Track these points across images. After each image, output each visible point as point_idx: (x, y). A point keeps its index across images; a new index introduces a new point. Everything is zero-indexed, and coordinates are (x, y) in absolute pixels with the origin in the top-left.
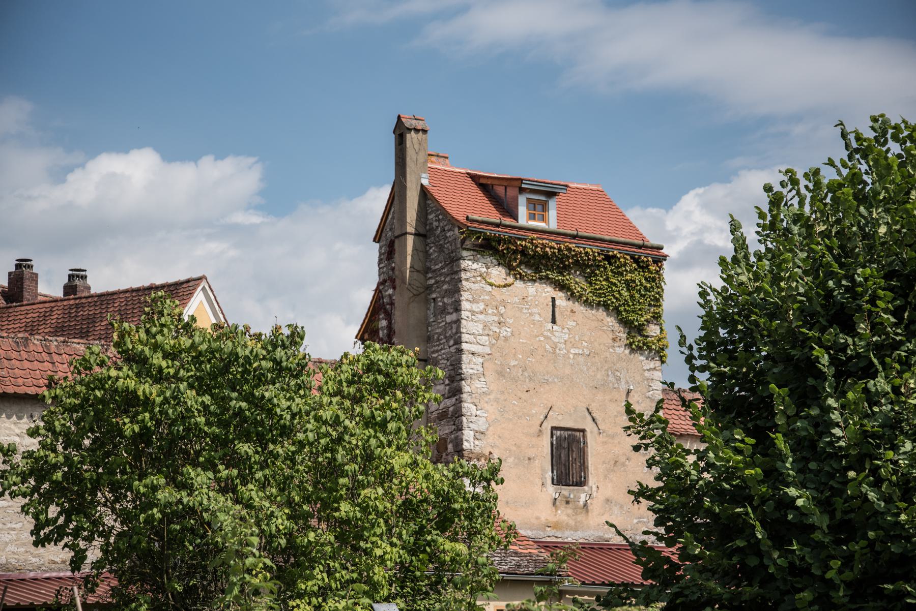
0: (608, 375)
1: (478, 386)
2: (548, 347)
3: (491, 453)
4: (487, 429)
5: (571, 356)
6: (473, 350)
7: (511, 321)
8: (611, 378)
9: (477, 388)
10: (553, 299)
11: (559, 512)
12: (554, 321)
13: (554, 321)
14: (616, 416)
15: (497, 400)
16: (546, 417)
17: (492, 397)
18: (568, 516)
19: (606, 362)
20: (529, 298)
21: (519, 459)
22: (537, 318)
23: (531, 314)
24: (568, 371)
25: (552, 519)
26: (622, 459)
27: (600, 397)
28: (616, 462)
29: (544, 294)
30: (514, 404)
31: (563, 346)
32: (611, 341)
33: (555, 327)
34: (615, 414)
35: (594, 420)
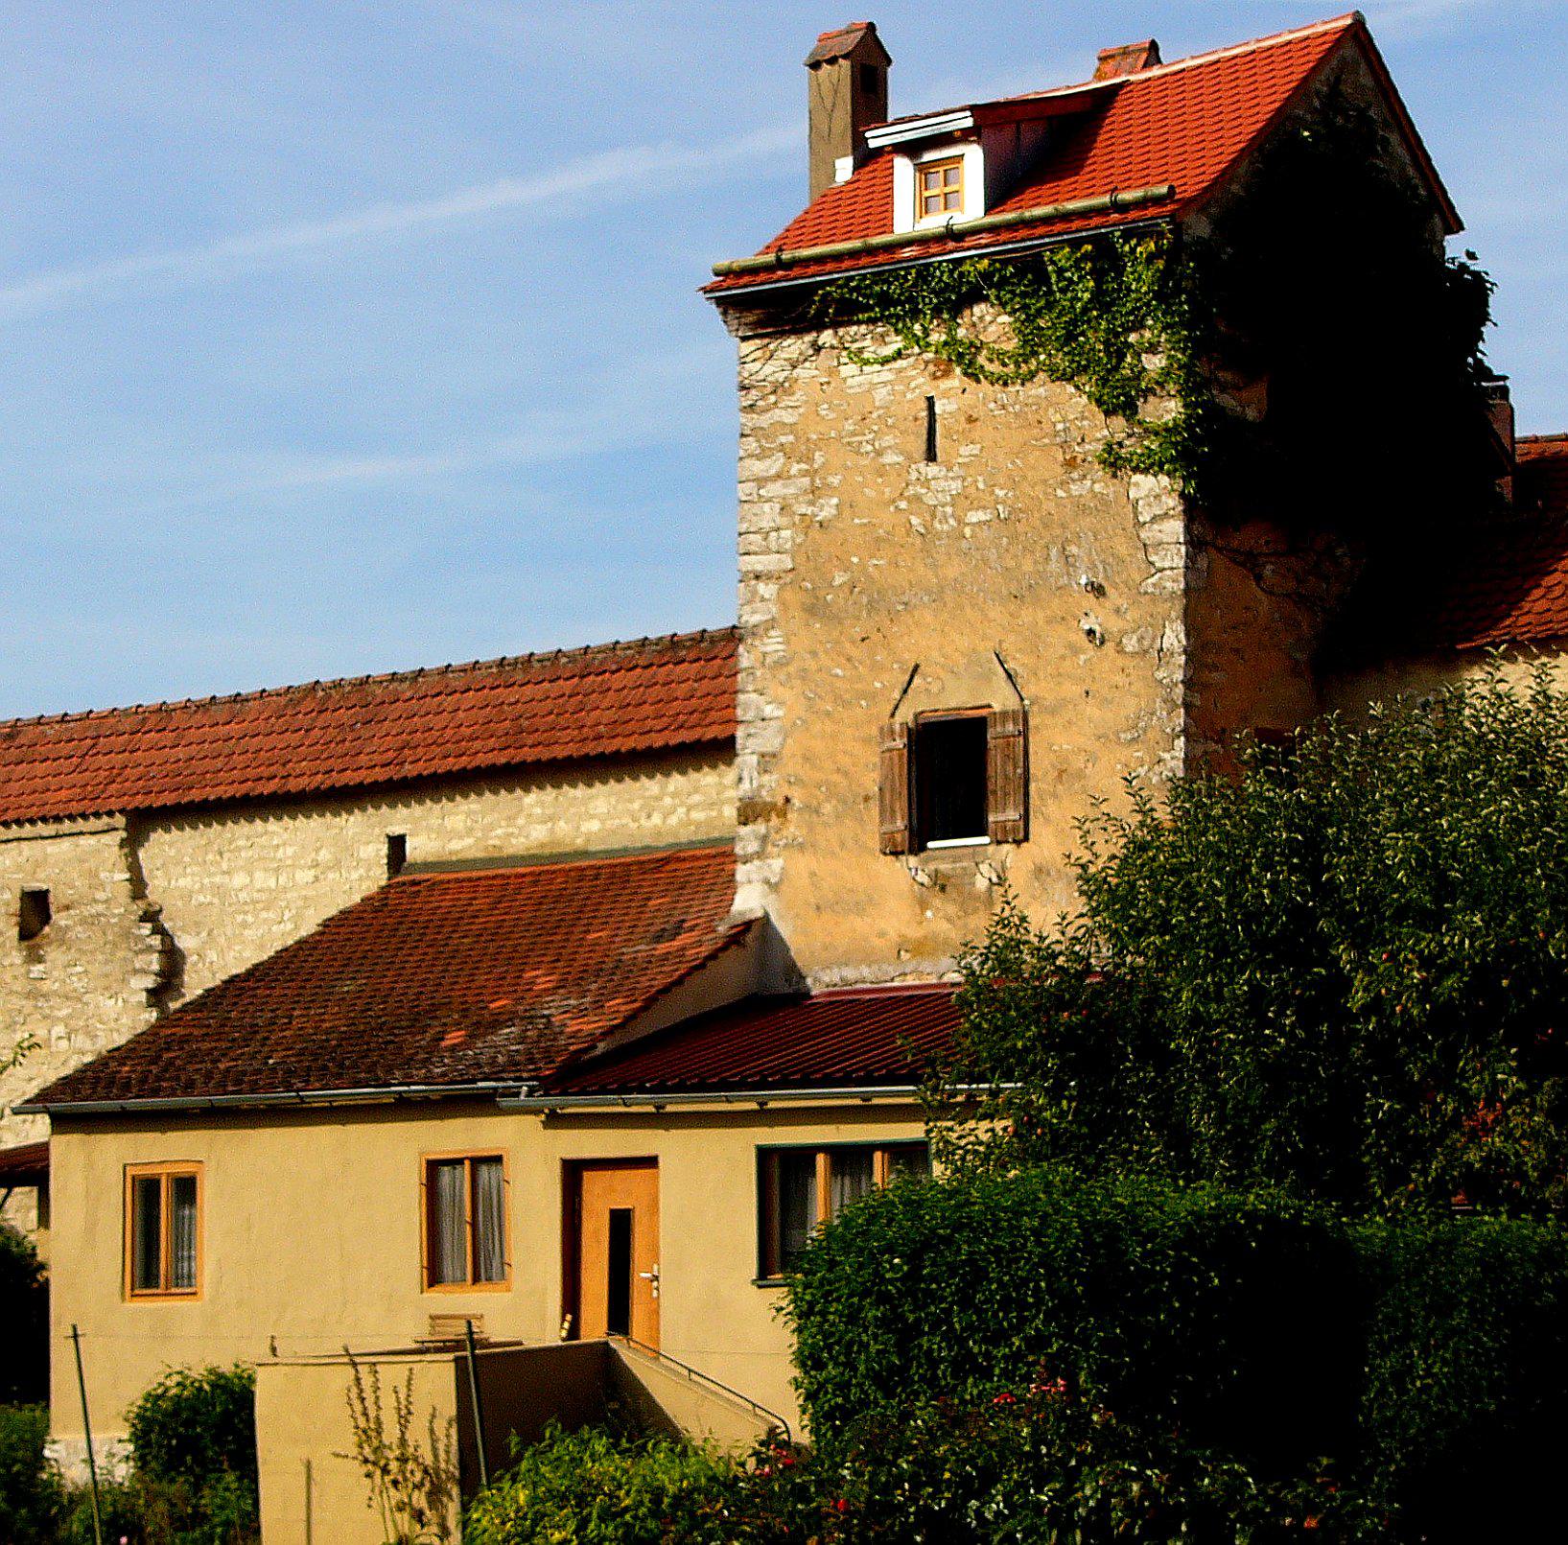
0: (1047, 558)
1: (769, 649)
2: (915, 521)
3: (787, 800)
4: (782, 745)
5: (968, 531)
6: (759, 568)
7: (835, 480)
8: (1055, 565)
9: (765, 654)
10: (930, 401)
11: (929, 914)
12: (931, 456)
13: (931, 456)
14: (1063, 658)
15: (804, 675)
16: (905, 691)
17: (791, 669)
18: (949, 920)
19: (1046, 526)
20: (875, 415)
21: (845, 803)
22: (890, 458)
23: (879, 453)
24: (952, 571)
25: (914, 933)
26: (1078, 762)
27: (1027, 615)
28: (1061, 772)
29: (909, 396)
30: (837, 676)
31: (949, 510)
32: (1060, 470)
33: (933, 470)
34: (1062, 651)
35: (1009, 676)
